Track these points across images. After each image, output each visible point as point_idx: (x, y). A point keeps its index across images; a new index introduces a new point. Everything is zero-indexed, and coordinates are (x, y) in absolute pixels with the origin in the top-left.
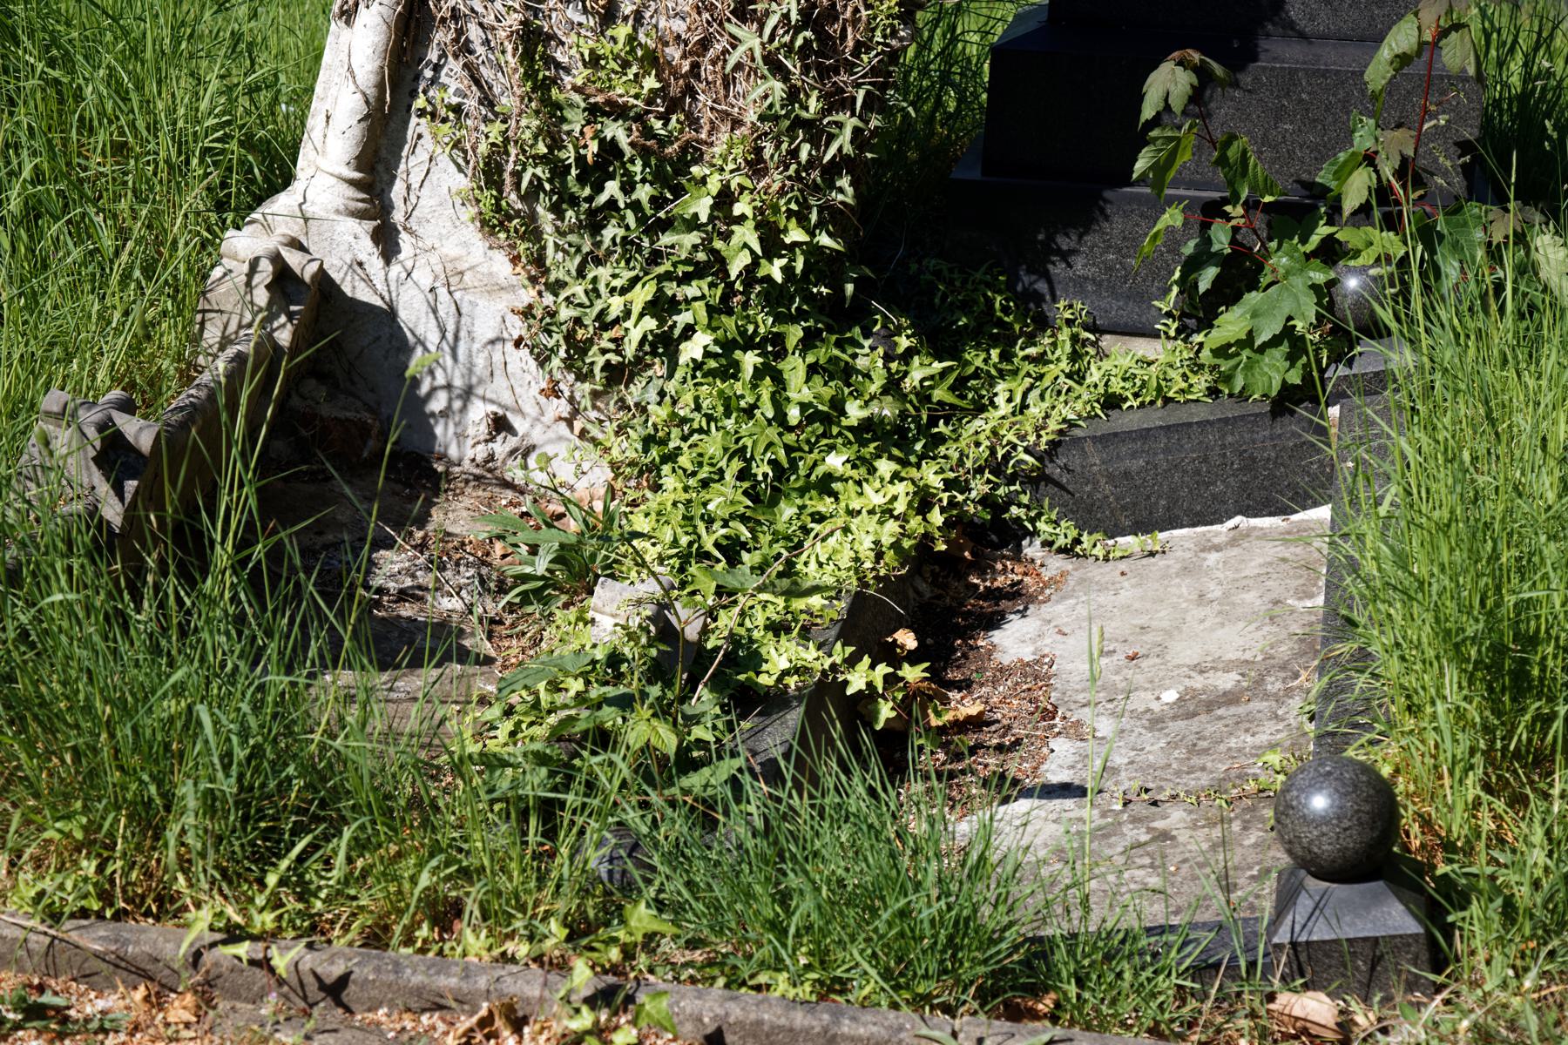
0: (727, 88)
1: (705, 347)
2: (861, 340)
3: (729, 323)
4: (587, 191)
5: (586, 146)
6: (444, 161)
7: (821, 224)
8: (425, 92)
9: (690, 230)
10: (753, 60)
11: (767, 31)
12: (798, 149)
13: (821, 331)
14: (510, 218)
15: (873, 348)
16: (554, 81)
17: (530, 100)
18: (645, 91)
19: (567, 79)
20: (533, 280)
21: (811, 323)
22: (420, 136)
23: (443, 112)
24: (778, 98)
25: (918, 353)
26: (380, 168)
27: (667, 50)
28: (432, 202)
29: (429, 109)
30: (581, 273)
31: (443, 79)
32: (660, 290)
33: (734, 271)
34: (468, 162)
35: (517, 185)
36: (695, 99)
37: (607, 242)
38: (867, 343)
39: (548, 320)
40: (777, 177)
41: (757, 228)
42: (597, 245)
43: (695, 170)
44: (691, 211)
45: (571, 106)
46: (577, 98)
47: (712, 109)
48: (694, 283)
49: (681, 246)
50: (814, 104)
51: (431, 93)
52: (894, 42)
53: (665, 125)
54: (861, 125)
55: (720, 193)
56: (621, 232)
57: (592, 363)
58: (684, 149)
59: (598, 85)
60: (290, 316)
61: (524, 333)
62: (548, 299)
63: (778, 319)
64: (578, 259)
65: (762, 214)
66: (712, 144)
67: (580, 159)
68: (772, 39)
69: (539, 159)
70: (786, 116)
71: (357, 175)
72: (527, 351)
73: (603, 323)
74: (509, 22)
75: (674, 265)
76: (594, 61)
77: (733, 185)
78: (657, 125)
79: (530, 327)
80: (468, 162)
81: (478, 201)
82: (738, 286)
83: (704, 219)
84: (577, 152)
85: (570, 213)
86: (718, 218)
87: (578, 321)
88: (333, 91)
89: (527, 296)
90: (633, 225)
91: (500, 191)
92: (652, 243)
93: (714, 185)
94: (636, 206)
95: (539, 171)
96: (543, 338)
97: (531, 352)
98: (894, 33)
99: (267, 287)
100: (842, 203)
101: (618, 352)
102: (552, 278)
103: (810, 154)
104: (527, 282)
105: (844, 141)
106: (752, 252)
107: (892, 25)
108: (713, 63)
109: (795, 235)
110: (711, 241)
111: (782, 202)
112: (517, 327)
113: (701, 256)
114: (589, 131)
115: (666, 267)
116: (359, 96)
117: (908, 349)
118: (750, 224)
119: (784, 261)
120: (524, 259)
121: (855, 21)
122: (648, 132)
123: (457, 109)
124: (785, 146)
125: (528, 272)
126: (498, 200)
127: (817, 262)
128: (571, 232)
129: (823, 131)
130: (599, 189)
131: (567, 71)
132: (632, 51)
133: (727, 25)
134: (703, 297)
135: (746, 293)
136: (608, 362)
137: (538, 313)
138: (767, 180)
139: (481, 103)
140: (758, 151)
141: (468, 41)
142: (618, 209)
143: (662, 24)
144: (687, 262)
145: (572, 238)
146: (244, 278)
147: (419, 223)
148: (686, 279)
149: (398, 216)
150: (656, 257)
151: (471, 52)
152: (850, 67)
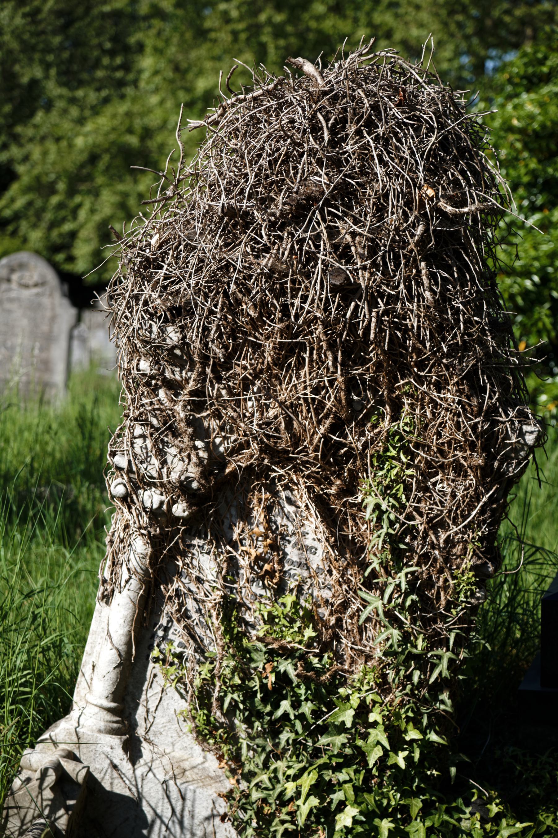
0: (361, 634)
1: (354, 817)
2: (464, 808)
3: (370, 798)
4: (269, 708)
5: (267, 677)
6: (171, 692)
7: (430, 726)
8: (158, 646)
9: (339, 734)
10: (378, 615)
11: (386, 596)
12: (411, 674)
13: (434, 802)
14: (217, 729)
15: (472, 814)
16: (244, 634)
17: (229, 648)
18: (306, 639)
19: (253, 633)
20: (233, 772)
21: (427, 797)
22: (155, 676)
23: (170, 658)
24: (396, 641)
25: (505, 816)
26: (129, 698)
27: (320, 610)
28: (164, 720)
29: (161, 657)
30: (266, 766)
31: (171, 636)
32: (320, 776)
33: (372, 761)
34: (187, 692)
35: (221, 707)
36: (339, 642)
37: (283, 743)
38: (468, 810)
39: (244, 801)
40: (398, 694)
41: (385, 730)
42: (276, 745)
43: (341, 691)
44: (340, 720)
45: (257, 650)
46: (260, 645)
47: (352, 648)
48: (344, 771)
49: (334, 745)
50: (420, 644)
51: (162, 646)
52: (473, 601)
53: (320, 661)
54: (453, 657)
55: (359, 706)
56: (292, 736)
57: (275, 831)
58: (334, 676)
59: (274, 636)
60: (67, 808)
61: (227, 810)
62: (244, 785)
63: (405, 795)
64: (263, 756)
65: (389, 719)
66: (352, 673)
67: (263, 687)
68: (390, 601)
69: (235, 688)
70: (402, 652)
71: (113, 705)
72: (230, 823)
73: (282, 801)
74: (214, 597)
75: (330, 758)
76: (271, 620)
77: (368, 700)
78: (315, 661)
79: (231, 806)
80: (187, 692)
81: (194, 718)
82: (374, 772)
83: (349, 725)
84: (261, 681)
85: (257, 724)
86: (358, 724)
87: (264, 800)
88: (97, 648)
89: (229, 784)
90: (300, 731)
91: (210, 711)
92: (314, 743)
93: (355, 701)
94: (301, 717)
95: (235, 696)
96: (241, 814)
97: (233, 824)
98: (473, 595)
99: (51, 788)
100: (444, 711)
101: (293, 822)
102: (246, 770)
103: (420, 677)
104: (228, 774)
105: (443, 668)
106: (383, 747)
107: (471, 590)
108: (351, 617)
109: (413, 734)
110: (354, 740)
111: (403, 711)
112: (223, 807)
113: (348, 751)
114: (269, 667)
115: (324, 760)
116: (114, 651)
117: (498, 813)
118: (381, 728)
119: (406, 753)
120: (226, 757)
121: (446, 587)
122: (308, 666)
123: (180, 656)
124: (402, 673)
125: (230, 766)
126: (208, 716)
127: (429, 753)
128: (258, 736)
129: (428, 662)
130: (276, 706)
131: (253, 627)
132: (297, 612)
133: (359, 592)
134: (351, 781)
135: (381, 776)
136: (286, 830)
137: (237, 796)
138: (391, 696)
139: (196, 651)
140: (384, 676)
141: (186, 610)
142: (289, 720)
143: (315, 593)
144: (339, 755)
145: (259, 741)
146: (37, 783)
147: (155, 735)
148: (338, 768)
149: (140, 731)
150: (317, 753)
151: (189, 618)
152: (444, 618)
